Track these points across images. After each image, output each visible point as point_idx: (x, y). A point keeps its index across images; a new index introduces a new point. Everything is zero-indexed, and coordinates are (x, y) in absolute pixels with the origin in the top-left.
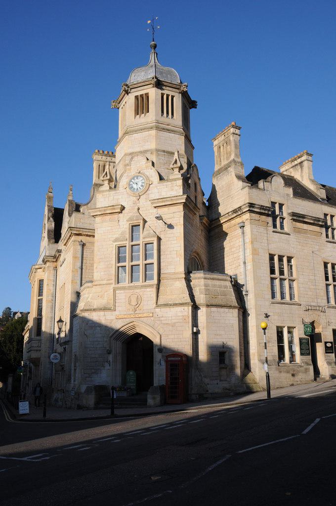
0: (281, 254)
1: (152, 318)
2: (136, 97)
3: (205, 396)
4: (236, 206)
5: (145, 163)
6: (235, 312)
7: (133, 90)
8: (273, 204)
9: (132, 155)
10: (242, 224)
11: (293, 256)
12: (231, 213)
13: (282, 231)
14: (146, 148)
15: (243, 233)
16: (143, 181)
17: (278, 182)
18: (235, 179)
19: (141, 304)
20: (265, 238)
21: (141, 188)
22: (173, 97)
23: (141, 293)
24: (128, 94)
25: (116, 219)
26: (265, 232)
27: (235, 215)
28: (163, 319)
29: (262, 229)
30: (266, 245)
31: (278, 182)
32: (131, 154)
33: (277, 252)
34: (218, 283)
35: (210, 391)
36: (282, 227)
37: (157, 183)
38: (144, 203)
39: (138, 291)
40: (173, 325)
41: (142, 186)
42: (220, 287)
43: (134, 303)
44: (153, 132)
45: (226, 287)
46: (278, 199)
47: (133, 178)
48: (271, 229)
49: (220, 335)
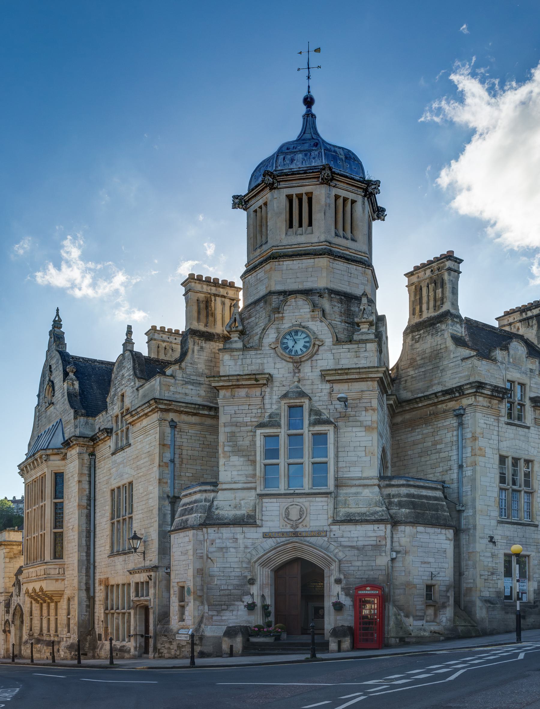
0: (516, 456)
1: (326, 539)
2: (290, 198)
3: (407, 640)
4: (451, 383)
5: (308, 310)
6: (450, 533)
7: (282, 184)
8: (512, 382)
9: (286, 294)
10: (462, 412)
11: (532, 459)
12: (440, 394)
13: (519, 423)
14: (308, 285)
15: (461, 424)
16: (307, 339)
17: (518, 349)
18: (450, 344)
19: (308, 518)
20: (495, 433)
21: (304, 350)
22: (353, 202)
23: (307, 504)
24: (271, 189)
25: (258, 394)
26: (496, 424)
27: (448, 397)
28: (342, 539)
29: (491, 420)
30: (496, 442)
31: (518, 349)
32: (280, 293)
33: (511, 454)
34: (424, 492)
35: (413, 635)
36: (520, 418)
37: (331, 344)
38: (310, 373)
39: (301, 500)
40: (358, 548)
41: (305, 346)
42: (426, 497)
43: (294, 515)
44: (323, 262)
45: (436, 499)
46: (515, 375)
47: (290, 333)
48: (505, 419)
49: (429, 563)
